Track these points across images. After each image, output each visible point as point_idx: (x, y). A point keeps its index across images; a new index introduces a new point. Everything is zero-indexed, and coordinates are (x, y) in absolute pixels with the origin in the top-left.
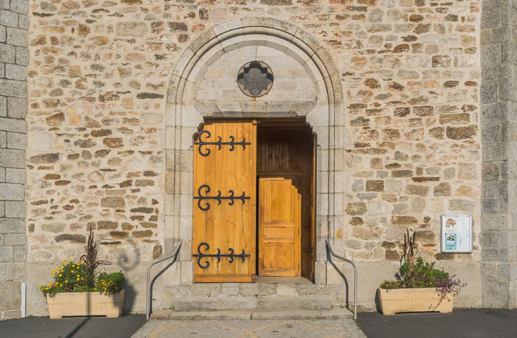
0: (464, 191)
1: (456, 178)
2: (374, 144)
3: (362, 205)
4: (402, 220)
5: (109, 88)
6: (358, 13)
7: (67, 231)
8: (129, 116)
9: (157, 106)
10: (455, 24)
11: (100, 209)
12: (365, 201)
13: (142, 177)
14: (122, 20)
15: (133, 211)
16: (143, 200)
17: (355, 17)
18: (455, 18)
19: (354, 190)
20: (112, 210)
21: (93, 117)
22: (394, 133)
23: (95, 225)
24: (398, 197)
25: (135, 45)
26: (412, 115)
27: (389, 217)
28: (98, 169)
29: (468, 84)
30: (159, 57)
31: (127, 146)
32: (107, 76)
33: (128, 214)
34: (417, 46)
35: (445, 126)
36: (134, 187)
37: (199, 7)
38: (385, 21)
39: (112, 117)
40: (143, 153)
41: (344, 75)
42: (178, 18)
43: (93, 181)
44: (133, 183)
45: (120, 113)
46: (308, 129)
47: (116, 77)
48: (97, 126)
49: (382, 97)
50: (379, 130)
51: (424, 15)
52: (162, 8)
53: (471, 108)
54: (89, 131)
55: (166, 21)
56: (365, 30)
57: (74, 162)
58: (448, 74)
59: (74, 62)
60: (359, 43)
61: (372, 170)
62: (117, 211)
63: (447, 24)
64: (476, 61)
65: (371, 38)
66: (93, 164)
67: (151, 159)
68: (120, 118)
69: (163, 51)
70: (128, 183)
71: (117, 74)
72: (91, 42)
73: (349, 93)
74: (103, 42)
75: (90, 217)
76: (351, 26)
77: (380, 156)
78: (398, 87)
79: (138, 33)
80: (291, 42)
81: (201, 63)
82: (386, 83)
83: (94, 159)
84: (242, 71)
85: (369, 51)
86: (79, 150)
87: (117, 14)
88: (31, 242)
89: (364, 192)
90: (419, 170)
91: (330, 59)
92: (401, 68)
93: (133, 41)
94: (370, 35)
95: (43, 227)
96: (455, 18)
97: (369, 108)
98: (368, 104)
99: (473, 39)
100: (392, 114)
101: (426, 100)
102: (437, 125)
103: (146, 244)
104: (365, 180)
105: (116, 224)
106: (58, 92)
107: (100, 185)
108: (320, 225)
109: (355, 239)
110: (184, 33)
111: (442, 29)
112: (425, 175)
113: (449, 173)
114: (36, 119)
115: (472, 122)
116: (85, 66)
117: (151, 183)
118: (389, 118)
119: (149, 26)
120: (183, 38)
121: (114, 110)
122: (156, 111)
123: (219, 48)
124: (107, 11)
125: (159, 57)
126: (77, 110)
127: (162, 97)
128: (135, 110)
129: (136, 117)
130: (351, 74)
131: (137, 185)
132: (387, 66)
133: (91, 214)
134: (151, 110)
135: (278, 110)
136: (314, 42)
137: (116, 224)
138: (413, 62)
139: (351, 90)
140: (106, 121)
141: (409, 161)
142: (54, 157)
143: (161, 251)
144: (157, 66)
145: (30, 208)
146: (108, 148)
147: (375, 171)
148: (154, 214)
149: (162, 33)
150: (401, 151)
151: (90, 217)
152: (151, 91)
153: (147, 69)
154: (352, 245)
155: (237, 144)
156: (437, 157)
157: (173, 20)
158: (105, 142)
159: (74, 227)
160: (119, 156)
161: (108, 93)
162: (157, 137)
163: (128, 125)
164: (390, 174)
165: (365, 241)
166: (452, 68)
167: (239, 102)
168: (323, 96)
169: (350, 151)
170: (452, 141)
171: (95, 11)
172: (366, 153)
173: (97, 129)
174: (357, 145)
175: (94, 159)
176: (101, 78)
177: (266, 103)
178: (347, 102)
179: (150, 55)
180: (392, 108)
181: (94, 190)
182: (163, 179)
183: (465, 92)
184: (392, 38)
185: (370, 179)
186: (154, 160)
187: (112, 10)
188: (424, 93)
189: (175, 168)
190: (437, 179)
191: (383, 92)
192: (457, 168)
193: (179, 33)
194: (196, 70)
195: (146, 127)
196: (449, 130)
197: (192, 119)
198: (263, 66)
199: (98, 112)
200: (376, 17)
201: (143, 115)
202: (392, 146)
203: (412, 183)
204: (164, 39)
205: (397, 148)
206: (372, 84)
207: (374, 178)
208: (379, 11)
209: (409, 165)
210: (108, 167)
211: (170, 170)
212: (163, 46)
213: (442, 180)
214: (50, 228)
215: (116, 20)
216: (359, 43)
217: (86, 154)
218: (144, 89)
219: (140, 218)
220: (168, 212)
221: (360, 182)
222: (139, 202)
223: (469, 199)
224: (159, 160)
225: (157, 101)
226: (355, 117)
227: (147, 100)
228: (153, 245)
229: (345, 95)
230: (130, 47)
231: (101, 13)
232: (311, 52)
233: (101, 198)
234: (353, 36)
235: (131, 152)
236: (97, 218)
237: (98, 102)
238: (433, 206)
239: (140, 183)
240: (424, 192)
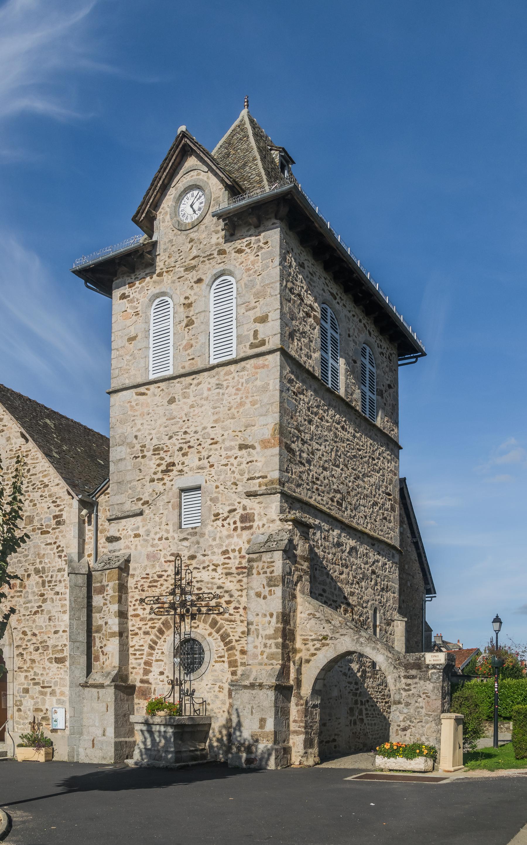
0: (62, 694)
1: (58, 687)
2: (25, 668)
3: (21, 701)
4: (37, 710)
6: (19, 594)
10: (58, 597)
17: (18, 597)
22: (33, 661)
26: (40, 651)
34: (42, 611)
35: (54, 656)
38: (31, 597)
49: (29, 641)
50: (27, 660)
51: (45, 593)
53: (65, 645)
58: (55, 626)
63: (54, 597)
77: (28, 674)
78: (34, 635)
94: (24, 606)
96: (57, 593)
99: (65, 605)
101: (46, 642)
102: (51, 656)
112: (46, 685)
113: (56, 683)
118: (31, 652)
132: (30, 623)
141: (39, 677)
166: (57, 623)
170: (57, 665)
178: (15, 645)
180: (32, 647)
188: (45, 638)
190: (50, 687)
191: (29, 638)
196: (56, 658)
202: (32, 668)
203: (41, 689)
205: (35, 669)
206: (24, 633)
207: (25, 686)
209: (39, 679)
213: (53, 688)
223: (64, 699)
238: (50, 702)
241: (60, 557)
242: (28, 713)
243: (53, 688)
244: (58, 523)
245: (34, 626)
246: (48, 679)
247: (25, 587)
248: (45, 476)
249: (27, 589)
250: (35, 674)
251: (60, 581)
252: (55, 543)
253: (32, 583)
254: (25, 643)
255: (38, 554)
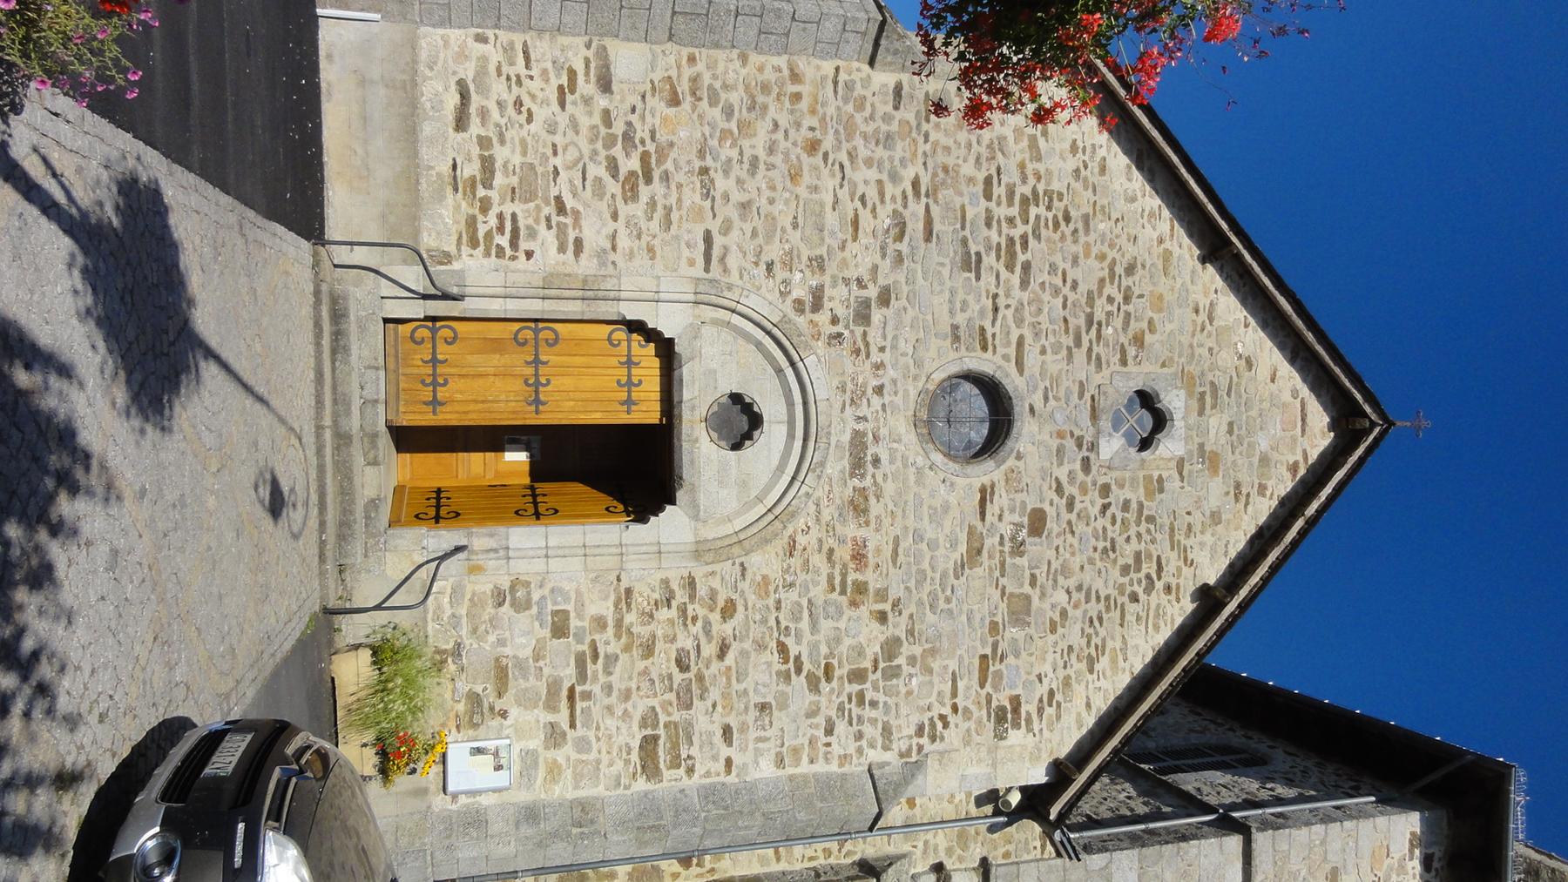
0: (554, 771)
1: (574, 756)
2: (630, 618)
3: (528, 606)
5: (722, 184)
7: (476, 101)
8: (675, 216)
9: (691, 263)
10: (821, 733)
11: (517, 160)
12: (535, 610)
13: (572, 235)
14: (828, 208)
15: (514, 216)
16: (532, 234)
17: (831, 578)
18: (829, 731)
19: (552, 591)
20: (515, 181)
21: (673, 154)
22: (649, 650)
23: (488, 149)
24: (541, 663)
25: (789, 228)
26: (678, 677)
27: (508, 651)
28: (587, 159)
29: (729, 762)
30: (770, 266)
31: (624, 210)
32: (739, 181)
33: (508, 209)
35: (661, 731)
36: (555, 219)
37: (846, 333)
38: (826, 625)
39: (673, 187)
40: (614, 237)
41: (742, 564)
42: (831, 299)
43: (565, 149)
44: (562, 219)
45: (679, 200)
46: (657, 509)
47: (737, 196)
48: (659, 162)
51: (835, 684)
52: (847, 274)
53: (690, 771)
54: (651, 147)
55: (827, 279)
56: (811, 595)
57: (597, 119)
58: (744, 728)
59: (763, 128)
60: (792, 585)
61: (588, 618)
62: (513, 190)
63: (820, 720)
64: (766, 769)
65: (799, 605)
66: (595, 152)
67: (604, 251)
68: (673, 200)
69: (780, 274)
70: (561, 209)
71: (744, 198)
72: (793, 157)
73: (713, 573)
74: (794, 177)
75: (502, 142)
76: (817, 572)
77: (610, 631)
78: (723, 651)
79: (808, 232)
80: (793, 478)
81: (759, 334)
82: (730, 632)
83: (603, 153)
84: (748, 400)
85: (779, 602)
86: (619, 128)
87: (836, 202)
88: (455, 34)
89: (550, 607)
90: (587, 696)
91: (767, 541)
92: (753, 655)
93: (795, 226)
94: (805, 603)
95: (484, 59)
96: (829, 731)
97: (690, 608)
98: (696, 606)
99: (797, 762)
100: (679, 644)
101: (702, 698)
102: (663, 718)
103: (455, 237)
104: (570, 607)
105: (491, 187)
106: (714, 100)
107: (558, 161)
108: (492, 536)
109: (468, 596)
110: (807, 309)
111: (812, 714)
112: (579, 705)
113: (583, 745)
114: (670, 58)
115: (667, 774)
116: (757, 144)
117: (562, 249)
118: (674, 640)
119: (818, 252)
120: (799, 306)
121: (685, 189)
122: (684, 261)
123: (784, 363)
124: (841, 186)
125: (770, 266)
126: (682, 129)
127: (707, 270)
128: (685, 226)
129: (674, 227)
130: (743, 575)
131: (558, 224)
132: (756, 631)
133: (508, 144)
134: (686, 253)
135: (686, 459)
136: (793, 515)
137: (491, 187)
138: (762, 673)
139: (718, 577)
140: (666, 177)
141: (602, 679)
142: (605, 85)
143: (442, 263)
144: (756, 264)
145: (518, 39)
146: (622, 178)
147: (586, 624)
148: (509, 252)
149: (808, 273)
150: (619, 664)
151: (502, 142)
152: (716, 252)
153: (750, 247)
154: (456, 593)
155: (629, 392)
156: (611, 723)
157: (828, 292)
158: (632, 173)
159: (484, 114)
160: (608, 196)
161: (712, 181)
162: (642, 260)
163: (659, 213)
164: (581, 648)
165: (464, 612)
166: (753, 734)
167: (699, 394)
168: (711, 532)
169: (619, 579)
171: (842, 167)
172: (616, 605)
173: (653, 161)
174: (629, 591)
175: (603, 153)
176: (736, 170)
177: (696, 440)
178: (699, 572)
179: (774, 252)
180: (689, 644)
181: (549, 152)
182: (568, 270)
183: (715, 758)
184: (799, 637)
185: (572, 615)
186: (601, 254)
187: (844, 194)
188: (714, 694)
189: (588, 290)
190: (573, 725)
191: (715, 629)
192: (593, 756)
193: (808, 299)
194: (750, 327)
195: (656, 242)
196: (656, 738)
197: (667, 322)
198: (756, 434)
199: (682, 163)
200: (831, 609)
201: (677, 238)
202: (627, 648)
203: (566, 685)
204: (798, 276)
205: (624, 657)
206: (728, 611)
207: (574, 623)
208: (840, 613)
209: (595, 678)
210: (590, 177)
211: (585, 281)
212: (787, 275)
213: (571, 734)
214: (481, 73)
215: (829, 199)
216: (792, 585)
217: (610, 142)
218: (718, 241)
219: (501, 229)
220: (512, 278)
221: (567, 600)
222: (528, 227)
223: (539, 781)
224: (603, 264)
225: (700, 261)
226: (675, 586)
227: (701, 247)
228: (452, 249)
229: (709, 568)
230: (786, 221)
231: (839, 175)
232: (777, 511)
233: (536, 163)
234: (802, 577)
235: (615, 216)
236: (500, 154)
237: (697, 164)
239: (562, 230)
240: (551, 707)
241: (920, 731)
242: (492, 638)
243: (571, 734)
244: (1000, 716)
245: (747, 645)
246: (596, 711)
247: (854, 604)
248: (1114, 661)
249: (848, 612)
250: (612, 659)
251: (859, 736)
252: (955, 709)
253: (865, 630)
254: (701, 612)
255: (933, 652)
